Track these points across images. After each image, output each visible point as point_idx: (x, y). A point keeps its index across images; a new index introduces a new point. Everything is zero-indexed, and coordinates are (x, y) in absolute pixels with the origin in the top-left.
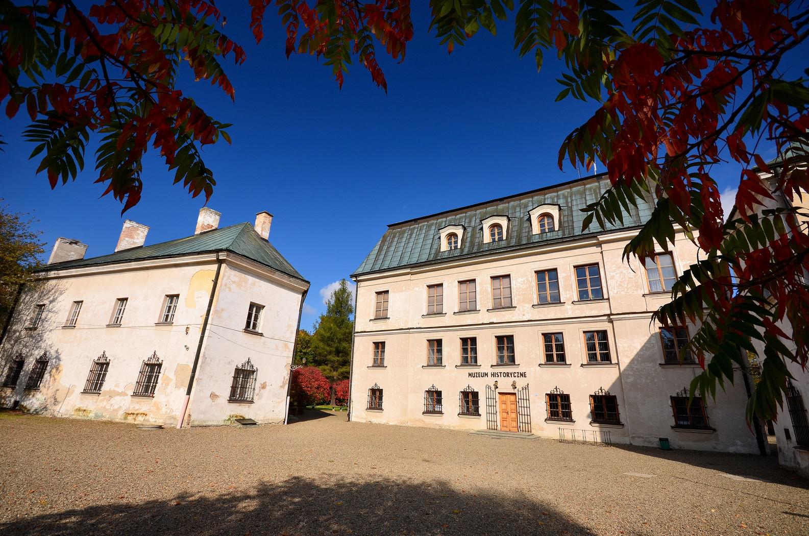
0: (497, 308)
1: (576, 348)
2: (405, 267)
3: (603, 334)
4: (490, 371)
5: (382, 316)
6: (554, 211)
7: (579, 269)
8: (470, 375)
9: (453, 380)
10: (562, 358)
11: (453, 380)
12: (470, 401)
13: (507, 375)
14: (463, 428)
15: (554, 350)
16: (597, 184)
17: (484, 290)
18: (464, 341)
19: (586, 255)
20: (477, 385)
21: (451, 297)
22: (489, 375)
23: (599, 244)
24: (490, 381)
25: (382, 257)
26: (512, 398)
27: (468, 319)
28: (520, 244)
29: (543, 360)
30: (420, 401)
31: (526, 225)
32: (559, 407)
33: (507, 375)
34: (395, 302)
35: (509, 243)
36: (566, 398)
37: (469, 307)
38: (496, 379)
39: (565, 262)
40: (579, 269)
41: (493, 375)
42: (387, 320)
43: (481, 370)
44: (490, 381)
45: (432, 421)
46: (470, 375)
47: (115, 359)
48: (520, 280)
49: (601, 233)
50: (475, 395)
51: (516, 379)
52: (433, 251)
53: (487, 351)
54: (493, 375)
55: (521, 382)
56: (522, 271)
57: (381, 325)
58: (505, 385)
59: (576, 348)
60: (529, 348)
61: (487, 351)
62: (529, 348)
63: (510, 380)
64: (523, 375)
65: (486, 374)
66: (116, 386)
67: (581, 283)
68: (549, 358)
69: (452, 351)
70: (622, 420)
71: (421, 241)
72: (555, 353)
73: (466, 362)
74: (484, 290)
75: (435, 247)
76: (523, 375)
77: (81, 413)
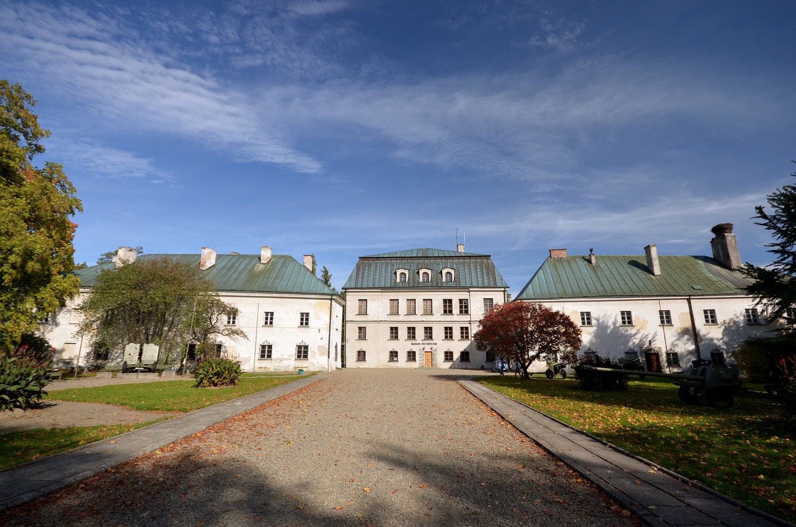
0: (425, 314)
1: (457, 333)
2: (378, 288)
3: (467, 328)
5: (363, 312)
6: (452, 272)
7: (461, 301)
9: (403, 345)
10: (451, 337)
11: (403, 345)
12: (412, 356)
13: (429, 344)
14: (408, 367)
16: (469, 260)
17: (420, 305)
18: (409, 328)
19: (464, 295)
20: (415, 348)
21: (403, 307)
23: (469, 292)
25: (360, 279)
26: (430, 353)
27: (412, 318)
28: (437, 287)
29: (444, 338)
30: (387, 356)
31: (440, 275)
32: (449, 356)
33: (429, 344)
34: (372, 307)
35: (432, 284)
37: (412, 311)
38: (424, 346)
39: (456, 297)
40: (461, 301)
41: (423, 344)
43: (417, 342)
44: (421, 347)
45: (393, 365)
47: (275, 343)
48: (436, 302)
49: (471, 287)
50: (414, 353)
52: (393, 281)
53: (420, 333)
54: (423, 344)
55: (434, 347)
56: (438, 298)
57: (363, 318)
58: (428, 348)
59: (457, 333)
60: (438, 333)
61: (420, 333)
62: (438, 333)
63: (431, 346)
65: (420, 344)
66: (281, 356)
67: (461, 307)
68: (446, 337)
69: (403, 333)
70: (470, 360)
73: (409, 338)
74: (420, 306)
75: (393, 278)
77: (263, 369)
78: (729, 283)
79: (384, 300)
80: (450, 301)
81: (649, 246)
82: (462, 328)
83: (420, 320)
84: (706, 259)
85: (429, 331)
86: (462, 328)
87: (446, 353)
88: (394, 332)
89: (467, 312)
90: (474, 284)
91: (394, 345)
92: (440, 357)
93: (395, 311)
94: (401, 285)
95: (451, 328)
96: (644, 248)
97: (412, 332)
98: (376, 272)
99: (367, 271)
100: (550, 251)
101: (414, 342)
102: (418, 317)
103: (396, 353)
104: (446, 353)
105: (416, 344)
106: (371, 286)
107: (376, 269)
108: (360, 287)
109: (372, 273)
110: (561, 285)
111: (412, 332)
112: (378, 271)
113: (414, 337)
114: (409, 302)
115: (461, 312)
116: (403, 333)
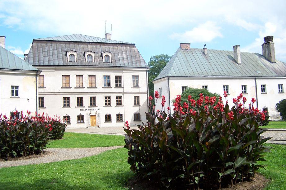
1: (113, 101)
4: (88, 108)
7: (116, 77)
8: (81, 110)
10: (109, 104)
12: (81, 118)
15: (108, 101)
20: (83, 113)
22: (88, 110)
24: (88, 112)
32: (108, 118)
36: (110, 116)
38: (90, 111)
39: (113, 75)
40: (116, 77)
41: (89, 110)
42: (45, 89)
43: (85, 108)
44: (88, 112)
46: (81, 110)
51: (97, 111)
53: (86, 102)
55: (98, 111)
56: (100, 75)
58: (93, 113)
59: (113, 101)
60: (100, 101)
61: (86, 102)
62: (100, 101)
63: (95, 111)
64: (98, 109)
65: (87, 110)
67: (116, 82)
68: (106, 104)
69: (73, 101)
71: (56, 53)
72: (108, 103)
76: (98, 109)
78: (272, 70)
79: (58, 76)
80: (109, 77)
81: (236, 46)
82: (117, 98)
83: (86, 92)
84: (259, 55)
85: (93, 101)
86: (117, 98)
87: (106, 116)
88: (67, 102)
89: (120, 85)
90: (126, 65)
91: (67, 112)
92: (103, 119)
93: (67, 85)
94: (71, 64)
95: (109, 98)
96: (233, 47)
97: (80, 101)
98: (49, 53)
99: (41, 52)
100: (180, 44)
101: (82, 108)
102: (86, 90)
103: (69, 117)
104: (106, 116)
105: (84, 110)
106: (47, 63)
107: (49, 50)
108: (38, 64)
109: (46, 53)
110: (190, 68)
111: (80, 101)
112: (51, 52)
113: (82, 105)
114: (78, 78)
115: (117, 85)
116: (73, 101)
